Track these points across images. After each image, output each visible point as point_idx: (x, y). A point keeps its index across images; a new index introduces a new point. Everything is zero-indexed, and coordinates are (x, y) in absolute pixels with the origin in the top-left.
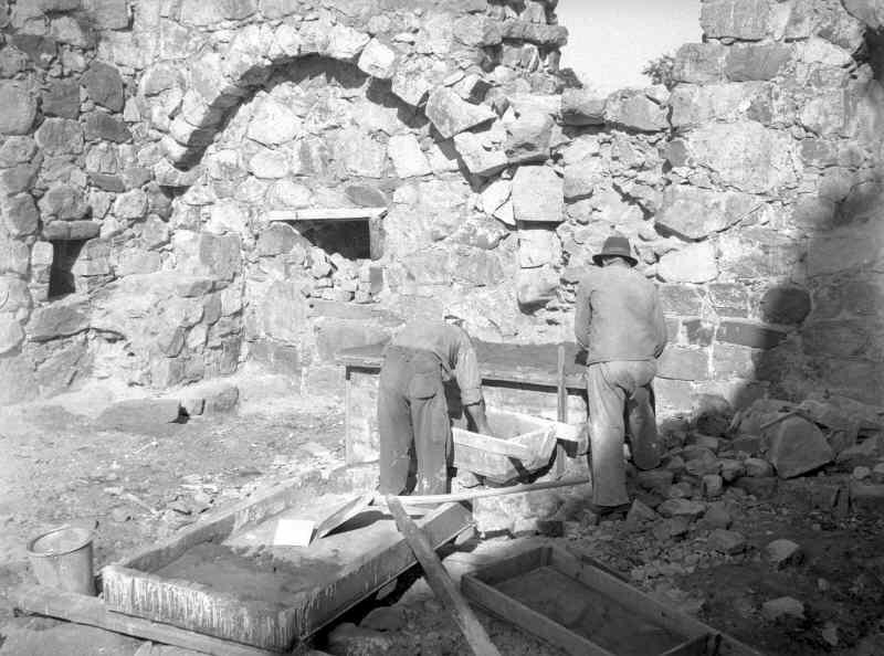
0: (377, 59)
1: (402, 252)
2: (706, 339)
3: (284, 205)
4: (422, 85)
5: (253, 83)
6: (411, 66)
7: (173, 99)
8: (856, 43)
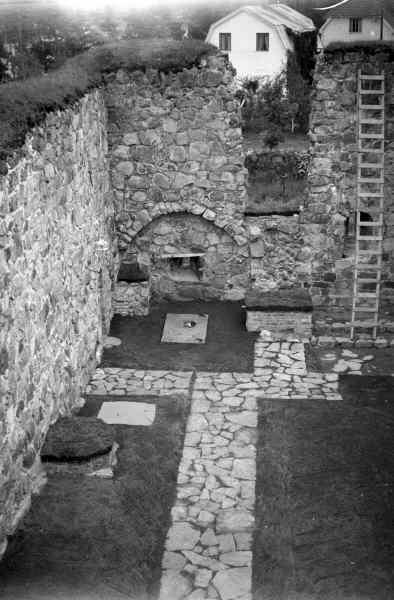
3: (165, 253)
4: (225, 222)
5: (157, 219)
6: (221, 217)
7: (129, 224)
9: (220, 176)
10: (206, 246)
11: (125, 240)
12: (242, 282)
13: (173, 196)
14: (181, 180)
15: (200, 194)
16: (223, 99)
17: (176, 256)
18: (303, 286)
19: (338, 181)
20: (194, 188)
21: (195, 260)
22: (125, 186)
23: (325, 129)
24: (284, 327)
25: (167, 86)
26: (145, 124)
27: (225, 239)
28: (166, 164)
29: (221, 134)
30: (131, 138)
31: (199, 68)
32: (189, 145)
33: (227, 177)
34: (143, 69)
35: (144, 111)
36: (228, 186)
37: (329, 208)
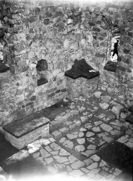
2: (24, 107)
8: (37, 63)
18: (21, 108)
19: (30, 45)
24: (37, 137)
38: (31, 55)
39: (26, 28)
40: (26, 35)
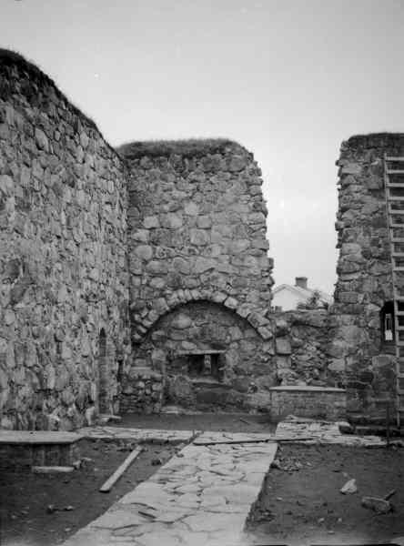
0: (232, 303)
1: (232, 365)
3: (184, 349)
4: (248, 311)
5: (175, 310)
6: (244, 305)
7: (144, 313)
8: (382, 305)
9: (243, 260)
10: (227, 341)
11: (139, 332)
12: (267, 384)
13: (194, 282)
14: (201, 264)
15: (221, 280)
16: (247, 182)
17: (194, 352)
19: (370, 267)
20: (214, 273)
21: (215, 358)
22: (143, 271)
23: (352, 213)
25: (190, 171)
26: (166, 207)
27: (249, 333)
28: (187, 248)
29: (245, 219)
30: (151, 221)
31: (223, 154)
32: (210, 228)
33: (250, 262)
34: (167, 155)
35: (166, 195)
36: (252, 271)
37: (361, 297)
38: (370, 286)
39: (364, 235)
40: (363, 248)
